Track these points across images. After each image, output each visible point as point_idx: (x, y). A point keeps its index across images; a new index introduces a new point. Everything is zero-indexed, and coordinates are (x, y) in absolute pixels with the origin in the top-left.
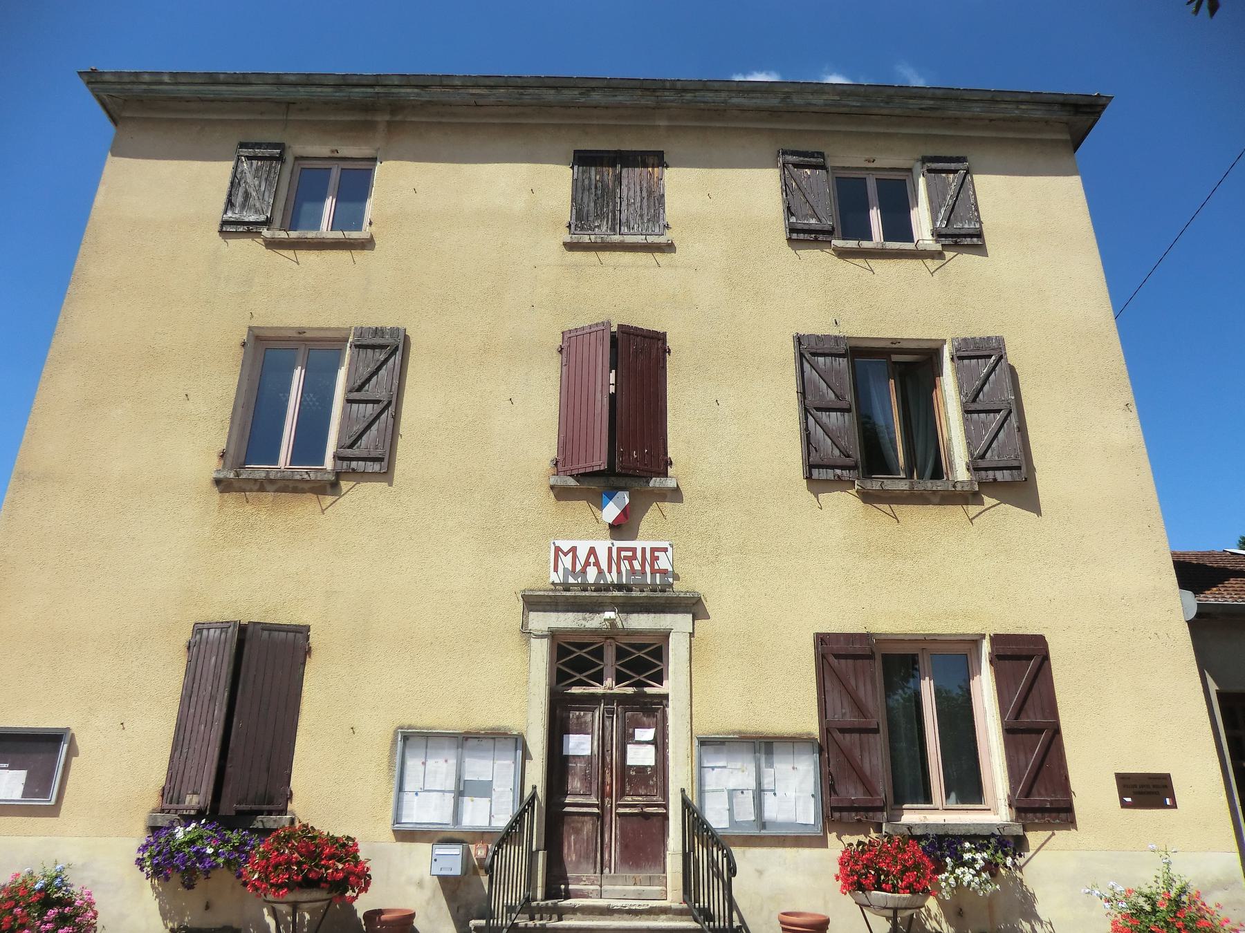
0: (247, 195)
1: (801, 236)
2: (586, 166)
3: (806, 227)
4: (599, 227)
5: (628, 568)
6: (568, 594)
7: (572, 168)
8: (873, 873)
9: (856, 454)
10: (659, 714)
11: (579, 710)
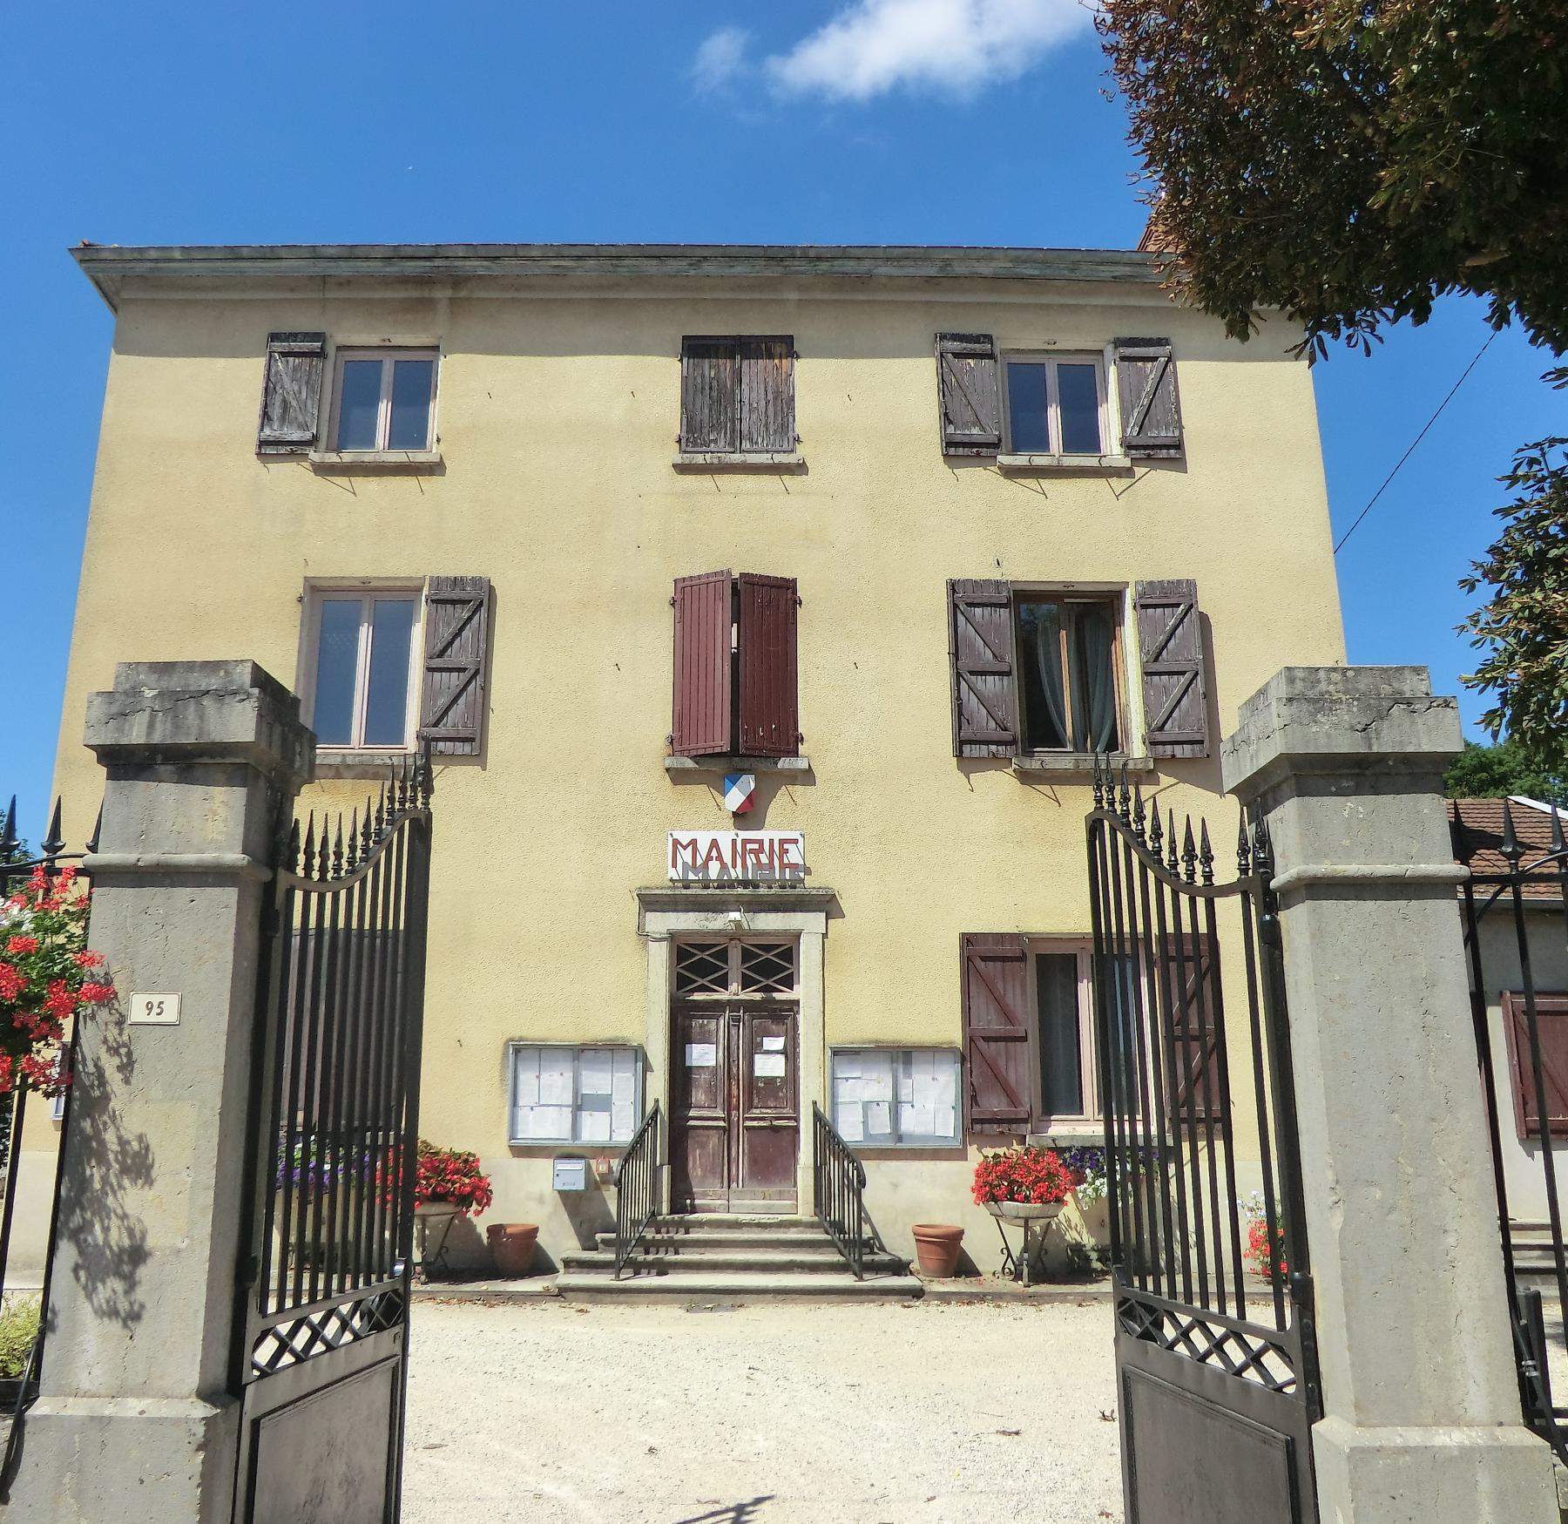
0: (285, 405)
1: (960, 451)
2: (698, 357)
3: (966, 440)
4: (715, 441)
5: (755, 862)
6: (688, 892)
7: (681, 360)
8: (1006, 1184)
9: (1016, 725)
10: (789, 1021)
11: (702, 1017)
